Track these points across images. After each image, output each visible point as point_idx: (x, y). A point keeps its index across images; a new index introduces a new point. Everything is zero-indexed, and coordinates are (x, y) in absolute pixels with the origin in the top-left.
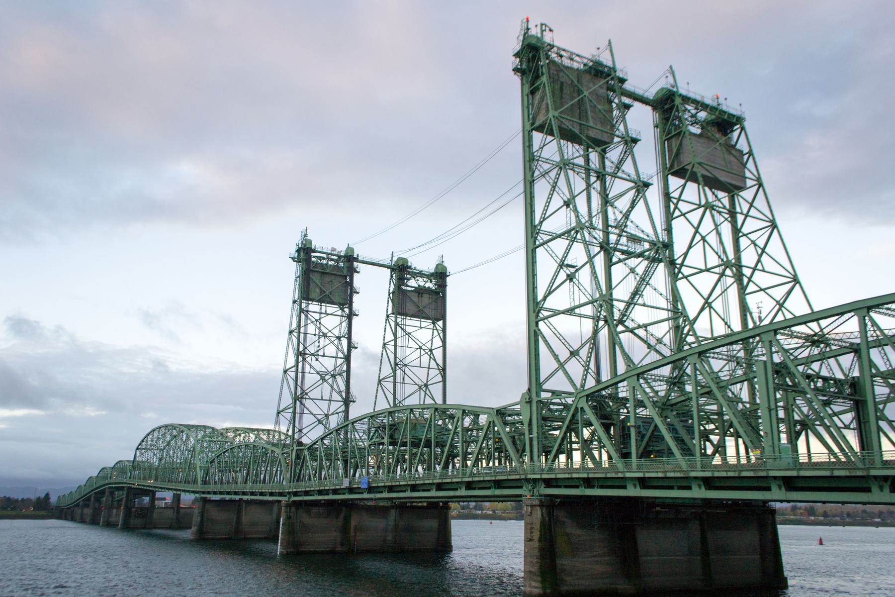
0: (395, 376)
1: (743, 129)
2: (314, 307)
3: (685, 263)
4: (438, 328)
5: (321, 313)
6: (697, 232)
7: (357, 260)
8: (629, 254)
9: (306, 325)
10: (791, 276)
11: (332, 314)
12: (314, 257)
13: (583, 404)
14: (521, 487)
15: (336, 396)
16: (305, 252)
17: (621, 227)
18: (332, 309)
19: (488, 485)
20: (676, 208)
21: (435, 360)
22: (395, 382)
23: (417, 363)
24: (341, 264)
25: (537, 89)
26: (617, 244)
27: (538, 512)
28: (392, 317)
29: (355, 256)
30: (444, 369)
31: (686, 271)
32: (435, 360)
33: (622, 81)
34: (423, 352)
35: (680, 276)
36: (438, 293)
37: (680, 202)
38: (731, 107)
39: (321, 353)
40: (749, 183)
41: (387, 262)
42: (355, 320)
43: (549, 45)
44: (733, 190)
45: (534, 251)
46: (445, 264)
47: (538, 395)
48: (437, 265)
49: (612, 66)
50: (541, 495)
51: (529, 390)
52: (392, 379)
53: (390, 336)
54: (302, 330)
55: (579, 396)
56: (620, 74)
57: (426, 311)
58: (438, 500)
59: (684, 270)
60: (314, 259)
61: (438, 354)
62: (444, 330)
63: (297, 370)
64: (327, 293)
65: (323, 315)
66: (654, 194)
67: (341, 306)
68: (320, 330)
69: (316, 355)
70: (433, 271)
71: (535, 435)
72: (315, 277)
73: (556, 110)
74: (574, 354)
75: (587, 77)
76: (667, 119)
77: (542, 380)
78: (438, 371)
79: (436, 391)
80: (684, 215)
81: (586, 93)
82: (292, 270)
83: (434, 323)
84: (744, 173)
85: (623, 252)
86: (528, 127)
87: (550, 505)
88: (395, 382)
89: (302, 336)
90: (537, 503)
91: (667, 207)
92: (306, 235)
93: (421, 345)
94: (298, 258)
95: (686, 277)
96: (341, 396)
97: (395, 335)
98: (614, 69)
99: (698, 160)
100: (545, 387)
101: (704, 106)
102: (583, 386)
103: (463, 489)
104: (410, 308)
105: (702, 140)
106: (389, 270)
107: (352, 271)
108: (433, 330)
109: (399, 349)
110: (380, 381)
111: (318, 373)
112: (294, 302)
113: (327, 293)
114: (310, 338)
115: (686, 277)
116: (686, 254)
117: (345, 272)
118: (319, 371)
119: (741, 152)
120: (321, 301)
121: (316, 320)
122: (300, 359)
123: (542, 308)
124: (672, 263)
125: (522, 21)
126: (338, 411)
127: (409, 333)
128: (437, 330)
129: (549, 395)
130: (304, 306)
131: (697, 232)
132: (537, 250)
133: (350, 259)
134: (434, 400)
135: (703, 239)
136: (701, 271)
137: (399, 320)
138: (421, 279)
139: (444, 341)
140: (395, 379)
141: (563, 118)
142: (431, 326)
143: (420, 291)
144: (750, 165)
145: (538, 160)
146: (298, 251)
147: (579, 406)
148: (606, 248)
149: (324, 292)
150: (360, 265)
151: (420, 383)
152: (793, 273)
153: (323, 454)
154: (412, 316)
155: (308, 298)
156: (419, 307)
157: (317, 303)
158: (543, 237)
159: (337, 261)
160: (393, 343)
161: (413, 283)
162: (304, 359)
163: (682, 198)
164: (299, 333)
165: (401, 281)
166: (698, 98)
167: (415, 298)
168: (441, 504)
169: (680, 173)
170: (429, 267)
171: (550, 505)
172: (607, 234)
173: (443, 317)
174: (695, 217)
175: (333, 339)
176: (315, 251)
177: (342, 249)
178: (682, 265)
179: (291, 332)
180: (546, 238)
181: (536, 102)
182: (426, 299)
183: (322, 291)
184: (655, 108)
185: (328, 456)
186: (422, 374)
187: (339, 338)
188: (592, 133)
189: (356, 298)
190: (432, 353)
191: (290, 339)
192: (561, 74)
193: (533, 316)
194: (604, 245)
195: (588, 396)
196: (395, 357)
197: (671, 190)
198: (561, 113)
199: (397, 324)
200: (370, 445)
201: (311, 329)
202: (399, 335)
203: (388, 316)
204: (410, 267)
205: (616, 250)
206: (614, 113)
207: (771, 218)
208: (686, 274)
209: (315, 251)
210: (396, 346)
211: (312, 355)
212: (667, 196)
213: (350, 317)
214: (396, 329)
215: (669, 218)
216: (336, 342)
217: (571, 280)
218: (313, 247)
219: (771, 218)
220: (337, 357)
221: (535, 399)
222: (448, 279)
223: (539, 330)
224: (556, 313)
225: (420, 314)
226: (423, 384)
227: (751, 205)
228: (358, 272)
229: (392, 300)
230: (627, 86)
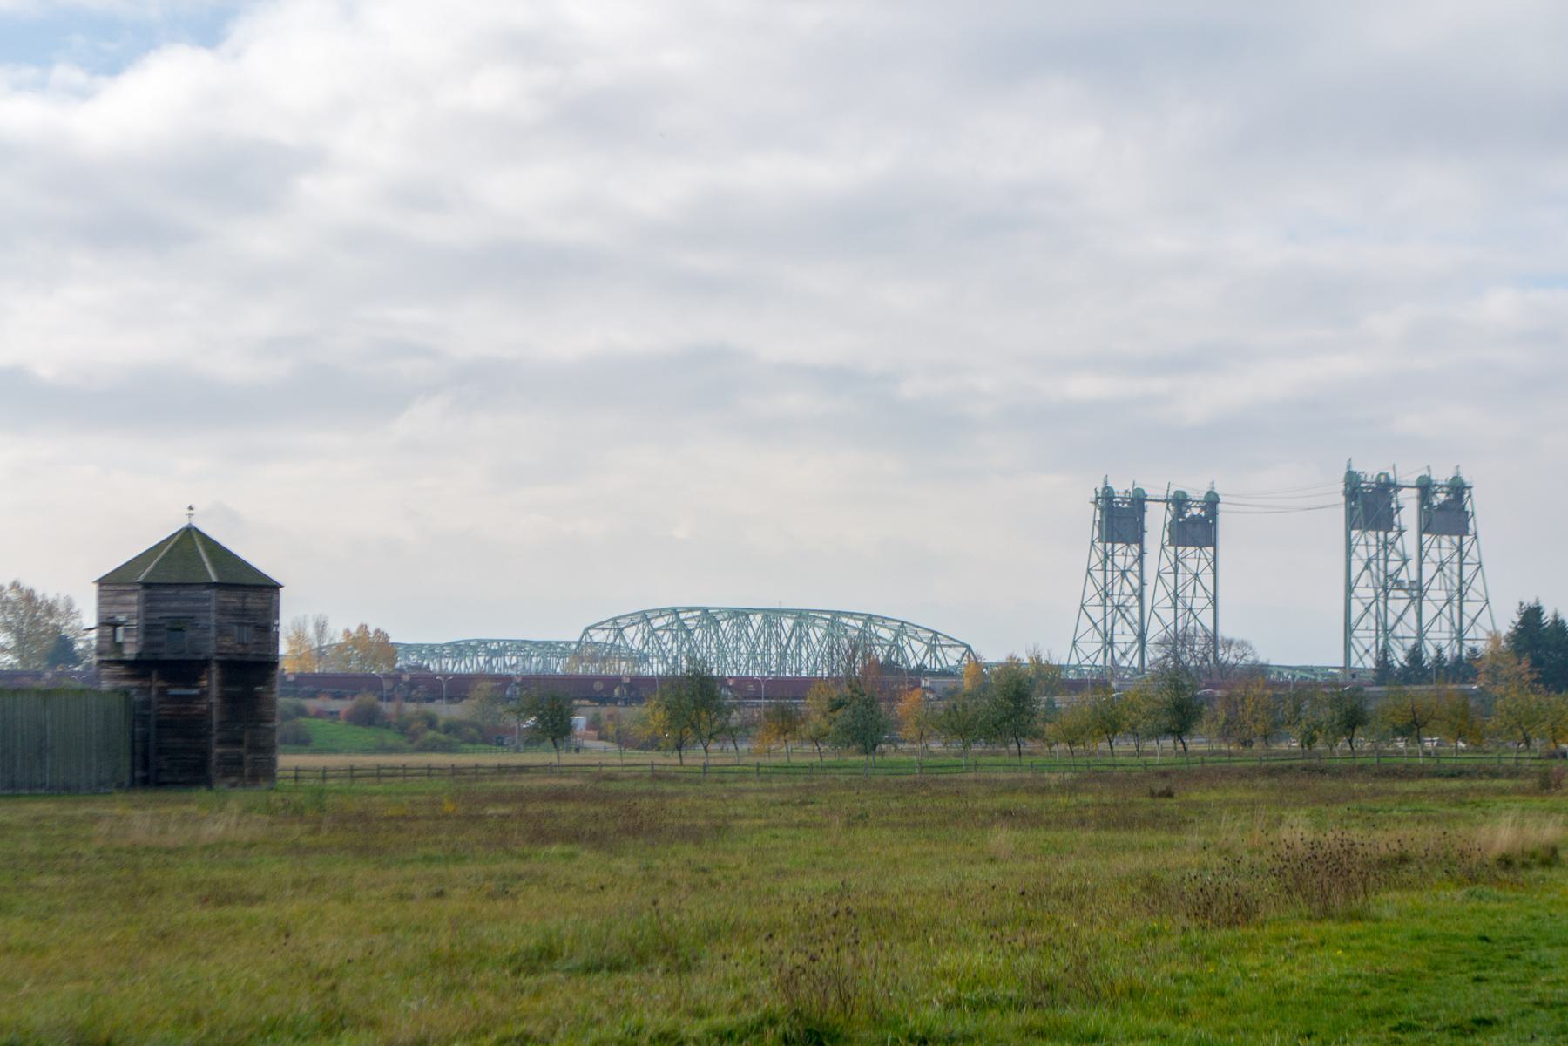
4: (1208, 556)
30: (1215, 598)
48: (1209, 493)
61: (1209, 583)
92: (1106, 483)
107: (1142, 510)
119: (1467, 512)
139: (1215, 571)
165: (1180, 513)
189: (1146, 536)
202: (1180, 571)
222: (1220, 507)
229: (1169, 531)
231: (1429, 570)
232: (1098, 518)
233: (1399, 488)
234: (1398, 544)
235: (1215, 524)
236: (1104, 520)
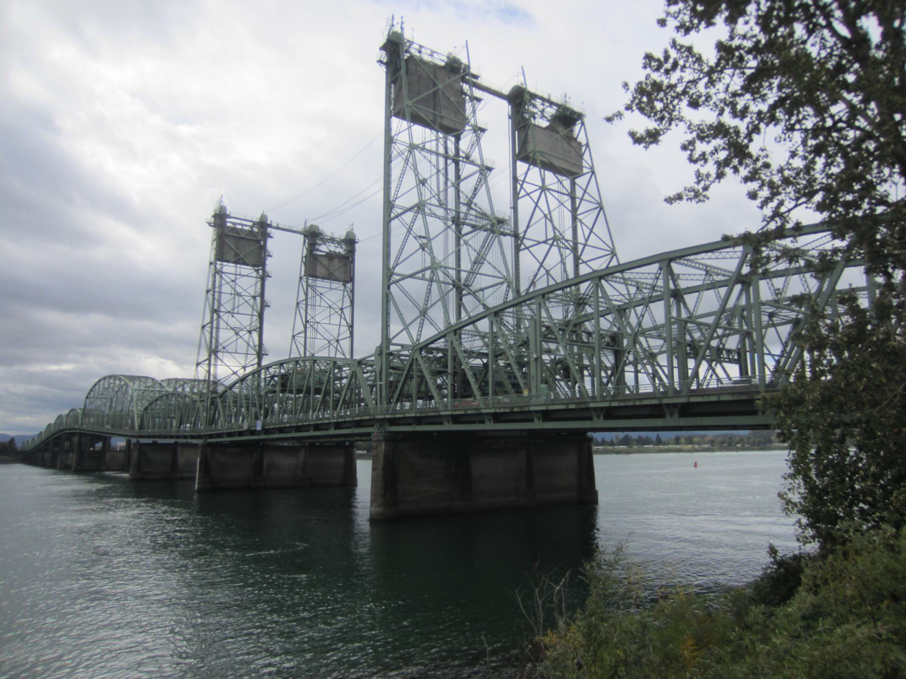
0: (305, 332)
1: (583, 124)
2: (229, 268)
3: (526, 237)
5: (236, 275)
7: (270, 226)
8: (475, 228)
9: (220, 286)
10: (609, 249)
11: (247, 276)
12: (231, 222)
13: (417, 356)
14: (372, 426)
17: (469, 205)
19: (349, 425)
20: (522, 187)
21: (345, 320)
22: (305, 337)
23: (327, 321)
24: (256, 230)
26: (466, 219)
27: (383, 446)
29: (269, 222)
31: (527, 243)
32: (345, 320)
33: (476, 77)
34: (332, 311)
35: (522, 247)
36: (348, 258)
37: (525, 184)
38: (575, 106)
39: (236, 311)
40: (585, 170)
42: (268, 281)
43: (409, 41)
44: (573, 175)
46: (355, 232)
47: (388, 348)
49: (467, 64)
50: (386, 432)
52: (303, 335)
53: (302, 297)
54: (217, 290)
55: (415, 348)
56: (473, 70)
57: (337, 274)
58: (342, 439)
59: (525, 241)
60: (229, 225)
61: (347, 312)
62: (352, 291)
63: (212, 326)
64: (241, 256)
65: (238, 277)
68: (235, 290)
69: (232, 313)
70: (343, 237)
71: (383, 383)
72: (230, 242)
73: (411, 98)
76: (518, 112)
77: (391, 336)
78: (347, 328)
79: (345, 344)
80: (528, 194)
81: (440, 86)
82: (209, 234)
83: (344, 285)
84: (582, 163)
85: (473, 226)
87: (393, 439)
88: (305, 337)
90: (382, 438)
91: (515, 188)
93: (331, 303)
94: (214, 223)
95: (527, 248)
97: (306, 294)
98: (468, 67)
99: (538, 148)
100: (394, 341)
101: (551, 104)
102: (418, 340)
103: (333, 429)
106: (302, 236)
107: (266, 236)
109: (309, 307)
110: (294, 336)
111: (232, 329)
112: (211, 263)
113: (241, 256)
114: (225, 298)
115: (527, 248)
116: (525, 232)
117: (259, 237)
118: (232, 326)
119: (580, 144)
120: (236, 262)
121: (233, 281)
122: (215, 316)
123: (393, 273)
124: (516, 236)
125: (388, 19)
126: (252, 363)
127: (321, 294)
129: (399, 348)
130: (218, 267)
132: (392, 222)
133: (263, 225)
134: (344, 355)
136: (539, 243)
137: (310, 282)
138: (332, 245)
139: (352, 302)
140: (306, 335)
141: (417, 108)
142: (342, 288)
143: (330, 256)
144: (586, 157)
145: (395, 143)
146: (215, 216)
147: (415, 358)
148: (457, 222)
149: (238, 255)
151: (329, 337)
152: (611, 246)
153: (231, 401)
154: (323, 278)
155: (222, 260)
156: (329, 270)
157: (233, 265)
158: (396, 211)
159: (252, 227)
160: (304, 302)
161: (324, 248)
162: (219, 317)
163: (526, 180)
164: (214, 292)
165: (312, 247)
166: (546, 96)
167: (325, 262)
168: (347, 444)
169: (525, 159)
170: (341, 234)
171: (393, 439)
173: (352, 280)
174: (535, 196)
175: (247, 299)
177: (256, 218)
178: (524, 238)
179: (208, 291)
180: (399, 211)
182: (336, 263)
184: (510, 103)
185: (235, 402)
186: (334, 330)
187: (254, 298)
188: (445, 122)
189: (269, 261)
190: (342, 312)
191: (207, 298)
192: (419, 68)
194: (456, 220)
195: (421, 349)
196: (306, 313)
198: (417, 102)
199: (308, 285)
200: (266, 393)
201: (226, 288)
203: (301, 278)
204: (321, 234)
205: (464, 224)
206: (467, 105)
207: (599, 201)
208: (528, 245)
209: (230, 217)
210: (307, 305)
211: (229, 312)
212: (515, 179)
213: (263, 278)
214: (307, 289)
215: (516, 196)
216: (251, 301)
217: (423, 249)
218: (228, 213)
219: (599, 201)
220: (252, 315)
221: (385, 352)
222: (357, 245)
223: (390, 293)
224: (404, 277)
225: (330, 277)
226: (333, 338)
227: (585, 191)
228: (272, 237)
230: (479, 81)
231: (525, 205)
233: (472, 80)
235: (353, 262)
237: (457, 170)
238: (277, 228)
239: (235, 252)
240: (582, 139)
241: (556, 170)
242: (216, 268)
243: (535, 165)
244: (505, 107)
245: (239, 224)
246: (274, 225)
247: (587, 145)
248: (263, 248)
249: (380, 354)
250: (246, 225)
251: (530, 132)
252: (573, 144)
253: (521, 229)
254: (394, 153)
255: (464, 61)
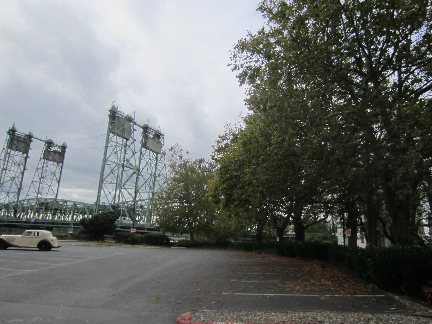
1: (163, 138)
2: (12, 152)
4: (60, 166)
6: (147, 163)
7: (33, 137)
15: (14, 186)
16: (12, 132)
18: (20, 153)
20: (143, 156)
22: (40, 183)
25: (114, 122)
28: (43, 160)
30: (59, 181)
36: (62, 154)
38: (162, 132)
41: (44, 139)
45: (104, 165)
46: (67, 144)
47: (99, 203)
48: (63, 144)
49: (133, 118)
51: (97, 201)
57: (56, 159)
59: (142, 173)
61: (58, 175)
62: (62, 167)
66: (137, 155)
67: (23, 153)
70: (61, 145)
72: (15, 142)
74: (110, 193)
75: (126, 121)
79: (55, 188)
81: (126, 126)
83: (58, 164)
86: (109, 132)
89: (6, 162)
91: (141, 156)
96: (17, 187)
98: (134, 120)
104: (51, 158)
105: (153, 140)
106: (44, 143)
107: (30, 141)
108: (57, 166)
109: (44, 172)
112: (4, 149)
119: (161, 144)
128: (59, 167)
130: (9, 151)
131: (147, 163)
133: (30, 137)
135: (148, 165)
139: (61, 171)
143: (55, 152)
144: (163, 148)
150: (34, 139)
154: (51, 160)
155: (11, 148)
158: (108, 162)
161: (53, 149)
165: (49, 147)
167: (53, 154)
169: (146, 148)
172: (124, 161)
173: (62, 162)
174: (147, 160)
176: (16, 131)
178: (142, 171)
181: (112, 126)
182: (57, 155)
183: (17, 147)
189: (30, 151)
193: (101, 183)
197: (143, 151)
199: (44, 163)
203: (41, 159)
209: (16, 131)
213: (26, 158)
222: (67, 150)
229: (44, 153)
231: (143, 163)
232: (8, 139)
234: (132, 147)
235: (64, 155)
236: (10, 139)
237: (125, 150)
238: (36, 138)
239: (16, 146)
240: (162, 142)
241: (153, 151)
242: (7, 152)
243: (148, 149)
244: (141, 130)
245: (20, 135)
246: (35, 137)
247: (164, 145)
248: (29, 145)
249: (96, 205)
250: (23, 136)
251: (148, 140)
252: (160, 144)
253: (141, 168)
254: (109, 145)
255: (133, 118)
